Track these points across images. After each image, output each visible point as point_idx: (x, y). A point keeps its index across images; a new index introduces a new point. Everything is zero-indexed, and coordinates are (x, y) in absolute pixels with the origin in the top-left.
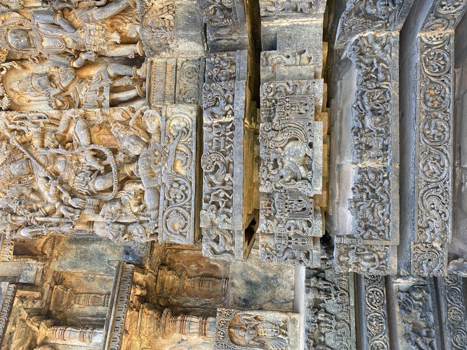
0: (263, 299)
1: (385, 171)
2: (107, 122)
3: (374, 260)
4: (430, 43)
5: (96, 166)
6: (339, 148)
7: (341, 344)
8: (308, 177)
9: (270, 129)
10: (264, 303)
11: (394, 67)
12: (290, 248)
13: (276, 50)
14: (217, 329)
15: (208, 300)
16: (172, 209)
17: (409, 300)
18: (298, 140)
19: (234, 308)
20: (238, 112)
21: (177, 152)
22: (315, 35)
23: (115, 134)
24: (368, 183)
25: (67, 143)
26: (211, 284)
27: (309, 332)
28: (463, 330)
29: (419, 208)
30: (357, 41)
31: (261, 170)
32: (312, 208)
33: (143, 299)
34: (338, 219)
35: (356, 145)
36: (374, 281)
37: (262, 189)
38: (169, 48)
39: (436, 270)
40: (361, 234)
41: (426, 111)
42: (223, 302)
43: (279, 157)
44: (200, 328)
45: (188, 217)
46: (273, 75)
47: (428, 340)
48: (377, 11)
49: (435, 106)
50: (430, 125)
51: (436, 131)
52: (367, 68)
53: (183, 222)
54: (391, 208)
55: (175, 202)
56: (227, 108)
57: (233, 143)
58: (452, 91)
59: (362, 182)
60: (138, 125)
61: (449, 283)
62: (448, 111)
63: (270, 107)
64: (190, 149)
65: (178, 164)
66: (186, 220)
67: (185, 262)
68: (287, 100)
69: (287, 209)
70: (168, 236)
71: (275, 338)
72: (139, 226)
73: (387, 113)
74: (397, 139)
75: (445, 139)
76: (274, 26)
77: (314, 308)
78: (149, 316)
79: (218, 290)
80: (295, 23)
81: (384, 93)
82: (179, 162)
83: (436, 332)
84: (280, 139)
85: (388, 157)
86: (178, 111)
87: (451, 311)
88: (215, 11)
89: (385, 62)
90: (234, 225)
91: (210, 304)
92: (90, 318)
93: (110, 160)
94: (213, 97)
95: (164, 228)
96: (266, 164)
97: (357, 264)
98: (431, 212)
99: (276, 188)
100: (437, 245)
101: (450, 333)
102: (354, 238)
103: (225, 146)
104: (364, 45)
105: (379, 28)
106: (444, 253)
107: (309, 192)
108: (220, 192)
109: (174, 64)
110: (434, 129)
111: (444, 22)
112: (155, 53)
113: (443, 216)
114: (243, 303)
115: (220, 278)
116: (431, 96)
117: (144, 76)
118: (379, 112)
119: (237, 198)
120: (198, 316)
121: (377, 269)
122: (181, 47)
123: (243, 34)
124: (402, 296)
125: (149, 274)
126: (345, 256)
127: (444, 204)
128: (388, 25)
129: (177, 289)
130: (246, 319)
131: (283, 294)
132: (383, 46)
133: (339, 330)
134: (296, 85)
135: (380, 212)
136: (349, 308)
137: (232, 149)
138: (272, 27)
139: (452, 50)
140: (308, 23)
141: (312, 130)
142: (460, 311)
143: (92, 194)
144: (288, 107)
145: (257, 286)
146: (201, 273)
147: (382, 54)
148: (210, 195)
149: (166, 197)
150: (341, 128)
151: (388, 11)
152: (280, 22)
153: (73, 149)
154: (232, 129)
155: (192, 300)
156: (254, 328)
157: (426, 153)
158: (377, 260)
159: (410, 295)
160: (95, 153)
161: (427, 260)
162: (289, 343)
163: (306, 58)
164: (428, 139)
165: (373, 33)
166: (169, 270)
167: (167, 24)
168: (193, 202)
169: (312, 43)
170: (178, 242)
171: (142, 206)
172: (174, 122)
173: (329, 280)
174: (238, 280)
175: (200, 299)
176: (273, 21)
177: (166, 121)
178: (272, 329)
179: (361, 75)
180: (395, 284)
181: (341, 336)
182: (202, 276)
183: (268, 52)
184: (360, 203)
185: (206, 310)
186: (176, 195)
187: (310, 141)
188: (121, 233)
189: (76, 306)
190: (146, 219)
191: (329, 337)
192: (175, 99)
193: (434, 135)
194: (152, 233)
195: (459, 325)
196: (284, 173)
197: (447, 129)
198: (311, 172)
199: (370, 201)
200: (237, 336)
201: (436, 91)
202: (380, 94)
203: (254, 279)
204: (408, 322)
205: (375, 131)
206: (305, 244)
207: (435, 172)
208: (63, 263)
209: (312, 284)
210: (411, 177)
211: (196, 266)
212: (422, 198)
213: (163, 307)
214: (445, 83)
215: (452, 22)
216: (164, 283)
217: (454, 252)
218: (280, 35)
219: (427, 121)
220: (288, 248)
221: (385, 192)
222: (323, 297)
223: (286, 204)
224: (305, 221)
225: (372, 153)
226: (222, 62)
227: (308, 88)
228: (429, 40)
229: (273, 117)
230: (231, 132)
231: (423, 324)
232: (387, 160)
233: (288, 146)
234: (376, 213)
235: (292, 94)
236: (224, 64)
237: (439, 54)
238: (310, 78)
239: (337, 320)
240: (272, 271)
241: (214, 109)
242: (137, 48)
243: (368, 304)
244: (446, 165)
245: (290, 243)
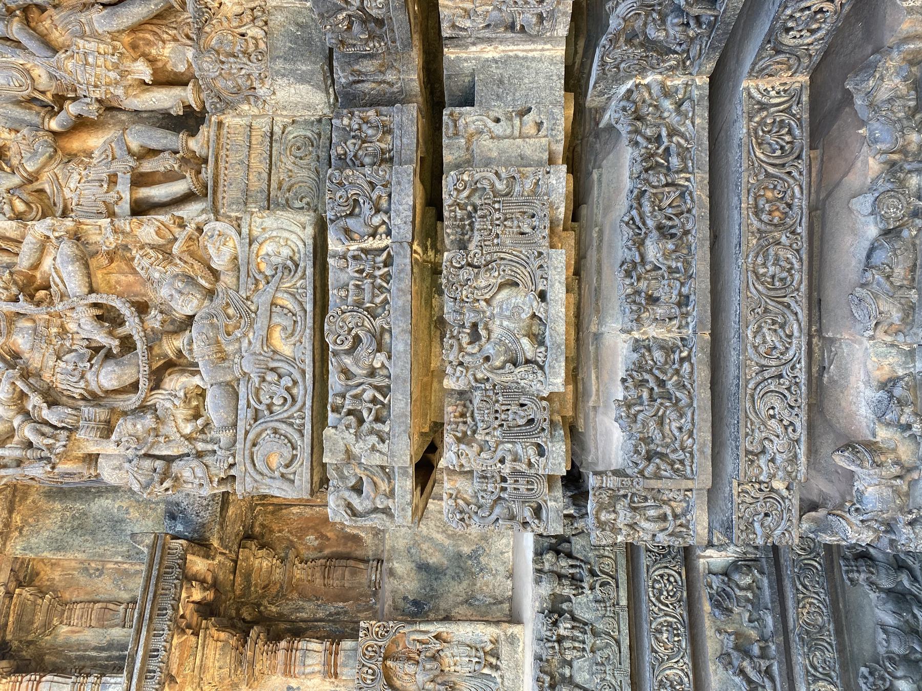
0: (451, 599)
1: (684, 346)
2: (126, 248)
3: (664, 518)
4: (764, 100)
5: (101, 338)
6: (597, 300)
7: (603, 680)
8: (538, 359)
9: (463, 263)
10: (455, 607)
11: (700, 145)
12: (504, 499)
13: (473, 106)
14: (360, 662)
15: (341, 604)
16: (264, 426)
17: (728, 589)
18: (517, 285)
19: (394, 620)
20: (399, 228)
21: (274, 309)
22: (549, 78)
23: (142, 273)
24: (651, 370)
25: (37, 290)
26: (347, 573)
27: (541, 660)
28: (827, 642)
29: (747, 417)
30: (630, 92)
31: (446, 346)
32: (545, 420)
33: (206, 610)
34: (596, 439)
35: (628, 296)
36: (664, 556)
37: (449, 383)
38: (255, 97)
39: (778, 532)
40: (640, 467)
41: (758, 230)
42: (371, 608)
43: (481, 320)
44: (326, 663)
45: (299, 443)
46: (468, 156)
47: (764, 664)
48: (667, 36)
49: (776, 221)
50: (766, 258)
51: (778, 269)
52: (650, 146)
53: (287, 453)
54: (696, 417)
55: (271, 413)
56: (376, 220)
57: (389, 291)
58: (805, 192)
59: (640, 367)
60: (192, 254)
61: (799, 555)
62: (799, 230)
63: (462, 220)
64: (301, 303)
65: (277, 334)
66: (294, 448)
68: (497, 206)
69: (497, 423)
70: (256, 481)
71: (475, 675)
72: (195, 463)
73: (687, 233)
74: (706, 284)
75: (794, 284)
76: (470, 58)
77: (550, 612)
78: (219, 644)
79: (361, 584)
80: (511, 54)
81: (682, 195)
82: (279, 329)
83: (777, 648)
84: (483, 284)
85: (689, 319)
86: (275, 226)
87: (804, 607)
88: (351, 24)
89: (682, 136)
90: (394, 456)
91: (346, 612)
92: (94, 654)
93: (132, 326)
94: (348, 198)
95: (248, 462)
96: (455, 333)
97: (632, 526)
98: (769, 423)
99: (476, 380)
100: (778, 485)
101: (803, 647)
102: (627, 476)
103: (374, 296)
104: (644, 102)
105: (672, 68)
106: (793, 501)
107: (541, 388)
108: (364, 391)
109: (267, 128)
110: (773, 264)
111: (791, 62)
112: (228, 105)
113: (790, 429)
114: (413, 608)
115: (365, 561)
116: (768, 201)
117: (204, 153)
118: (673, 231)
119: (400, 402)
120: (321, 639)
121: (670, 535)
122: (281, 95)
123: (407, 72)
124: (716, 582)
125: (219, 558)
126: (609, 512)
127: (792, 407)
128: (688, 63)
129: (278, 585)
130: (418, 641)
131: (491, 587)
132: (679, 104)
133: (599, 653)
134: (514, 177)
135: (675, 425)
136: (617, 609)
137: (388, 303)
138: (466, 60)
139: (806, 116)
140: (536, 54)
141: (545, 266)
142: (821, 605)
143: (93, 398)
144: (497, 219)
145: (439, 573)
146: (327, 552)
147: (678, 118)
148: (344, 397)
149: (252, 402)
150: (599, 261)
151: (688, 36)
152: (482, 51)
153: (51, 303)
154: (388, 263)
155: (310, 606)
156: (434, 658)
157: (759, 310)
158: (670, 518)
159: (729, 579)
160: (99, 312)
161: (763, 514)
162: (502, 683)
163: (532, 124)
164: (762, 283)
165: (659, 77)
166: (262, 547)
167: (251, 48)
168: (308, 412)
169: (543, 95)
170: (276, 493)
171: (200, 422)
172: (268, 248)
173: (578, 556)
175: (325, 604)
176: (467, 47)
177: (250, 245)
178: (470, 657)
179: (639, 159)
180: (702, 560)
181: (603, 664)
182: (329, 558)
183: (458, 110)
184: (638, 408)
185: (338, 626)
186: (271, 398)
187: (541, 288)
188: (157, 477)
189: (64, 629)
190: (210, 447)
191: (580, 668)
192: (269, 200)
193: (773, 277)
194: (222, 475)
195: (819, 632)
196: (491, 351)
197: (797, 266)
198: (543, 349)
199: (657, 404)
200: (401, 674)
201: (776, 192)
202: (673, 196)
203: (434, 559)
204: (726, 632)
205: (664, 268)
206: (533, 489)
207: (775, 348)
208: (33, 540)
209: (547, 566)
210: (733, 357)
211: (316, 539)
212: (752, 396)
213: (249, 622)
214: (793, 177)
215: (806, 61)
216: (250, 575)
217: (811, 497)
218: (481, 76)
219: (761, 250)
220: (500, 498)
221: (684, 386)
222: (567, 591)
223: (497, 411)
224: (533, 444)
225: (660, 311)
226: (364, 127)
227: (537, 184)
228: (764, 95)
229: (469, 240)
230: (386, 269)
231: (754, 634)
232: (687, 324)
233: (499, 297)
234: (667, 427)
235: (506, 195)
236: (370, 132)
237: (782, 121)
238: (539, 164)
239: (595, 634)
240: (468, 542)
241: (351, 223)
242: (188, 95)
243: (653, 599)
244: (796, 334)
245: (504, 489)
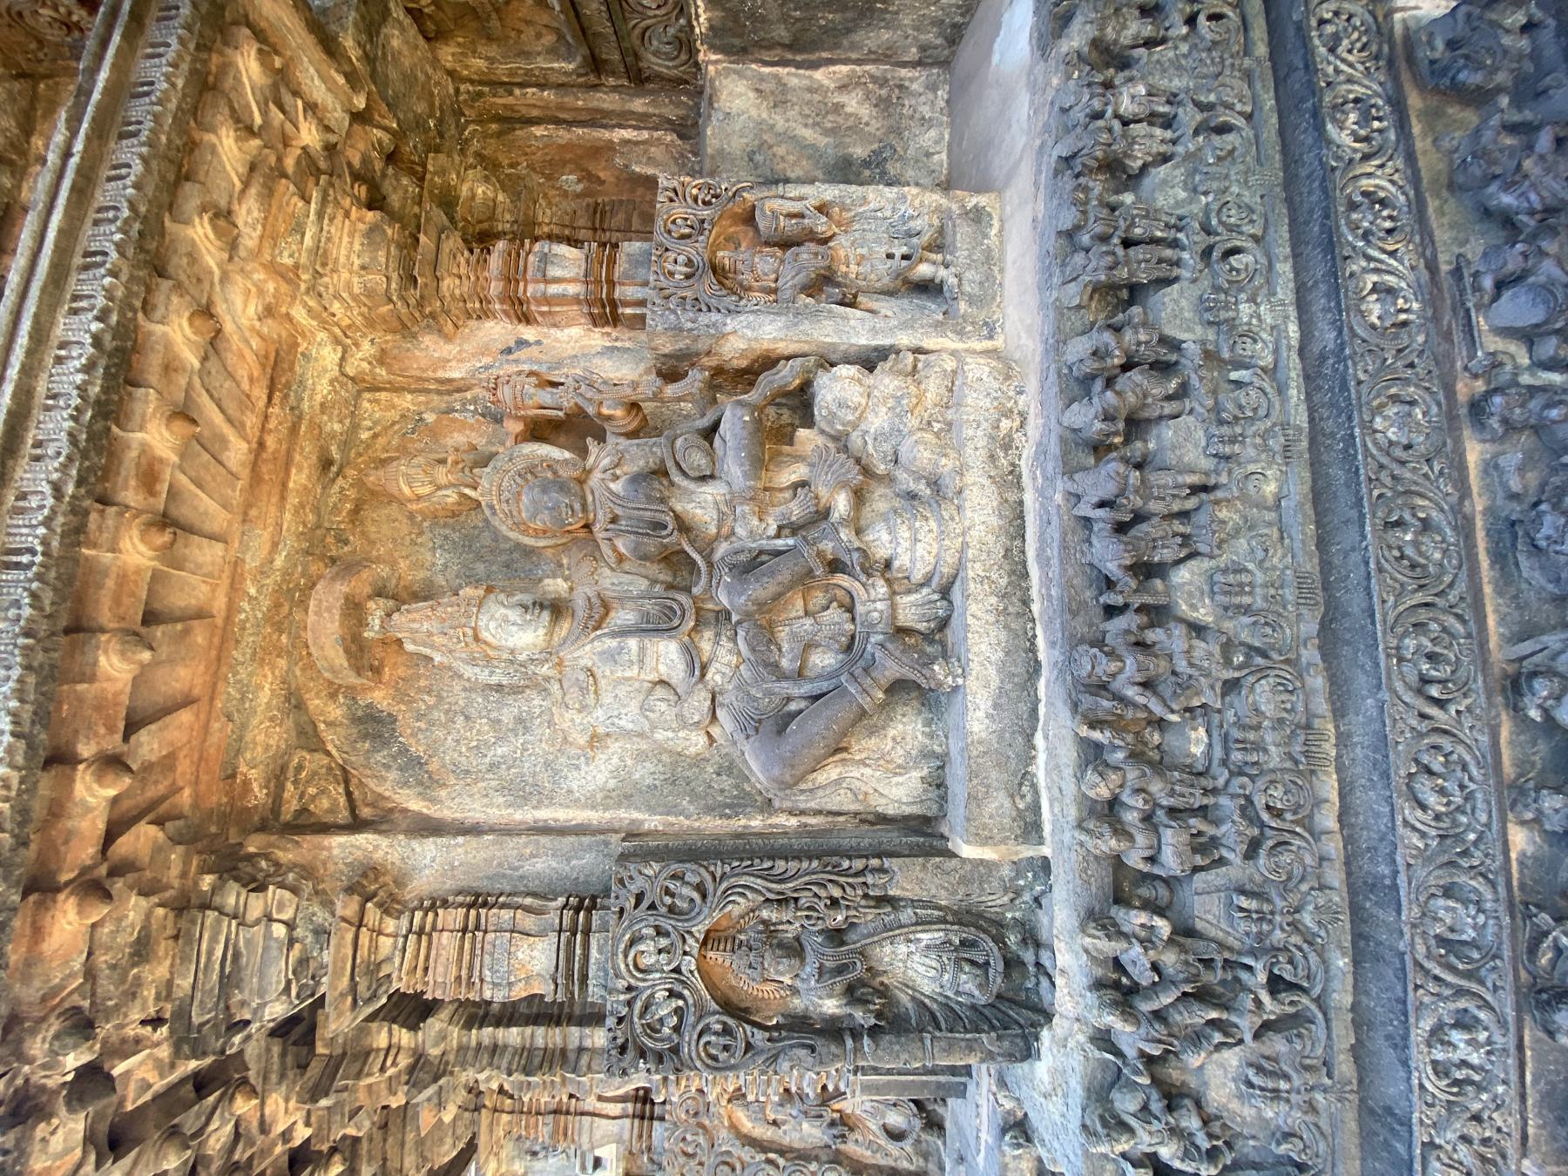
14: (661, 245)
162: (960, 285)
211: (579, 181)
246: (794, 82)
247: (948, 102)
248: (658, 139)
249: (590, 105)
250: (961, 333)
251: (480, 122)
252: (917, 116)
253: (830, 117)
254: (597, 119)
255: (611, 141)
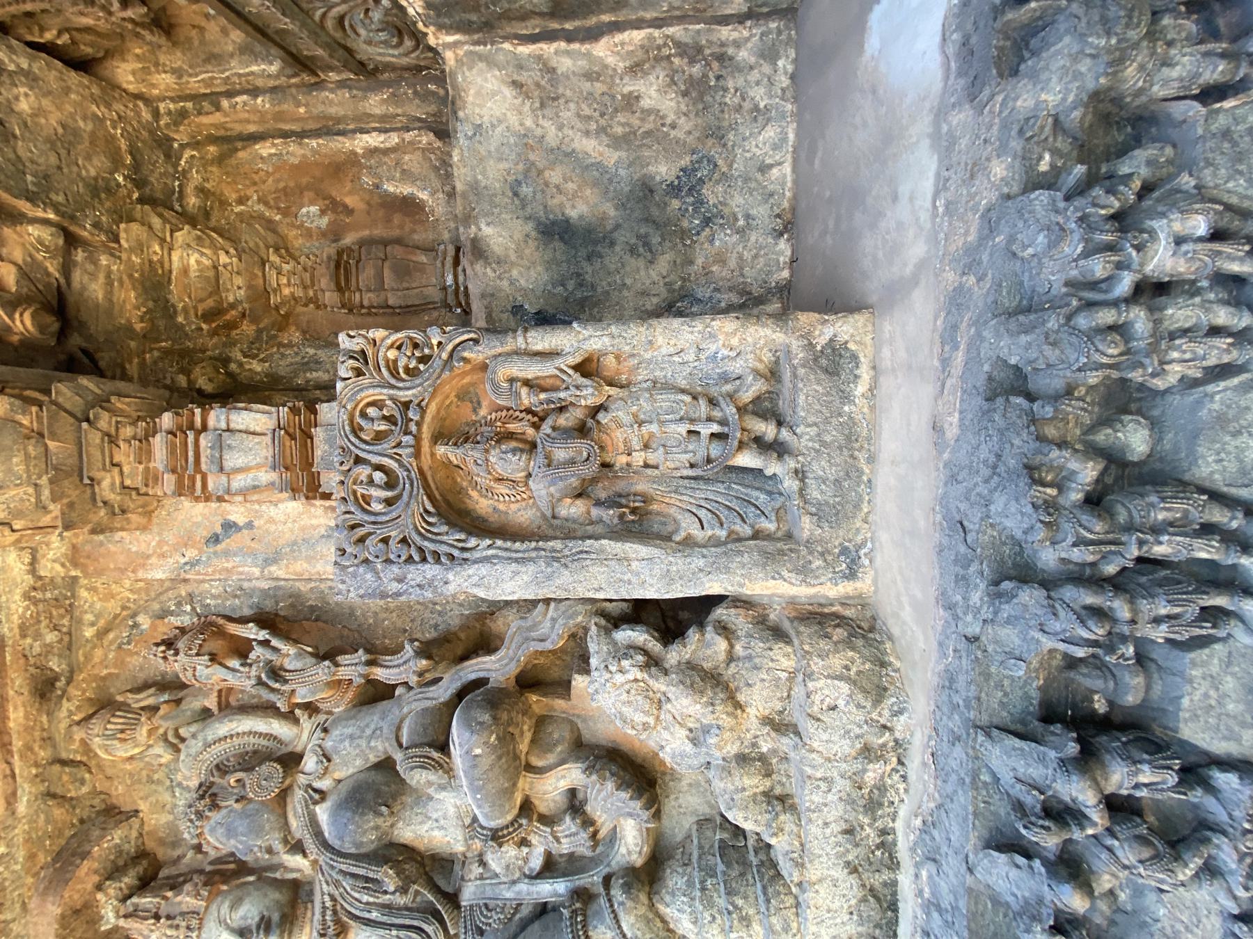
26: (387, 273)
44: (280, 463)
67: (270, 198)
130: (527, 383)
131: (732, 263)
145: (596, 242)
174: (501, 223)
178: (692, 421)
200: (483, 480)
211: (323, 212)
246: (565, 64)
247: (793, 77)
248: (411, 143)
249: (315, 111)
250: (804, 571)
251: (196, 145)
252: (747, 105)
253: (620, 118)
254: (329, 128)
255: (354, 153)
